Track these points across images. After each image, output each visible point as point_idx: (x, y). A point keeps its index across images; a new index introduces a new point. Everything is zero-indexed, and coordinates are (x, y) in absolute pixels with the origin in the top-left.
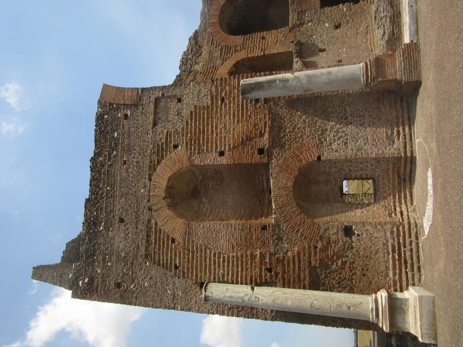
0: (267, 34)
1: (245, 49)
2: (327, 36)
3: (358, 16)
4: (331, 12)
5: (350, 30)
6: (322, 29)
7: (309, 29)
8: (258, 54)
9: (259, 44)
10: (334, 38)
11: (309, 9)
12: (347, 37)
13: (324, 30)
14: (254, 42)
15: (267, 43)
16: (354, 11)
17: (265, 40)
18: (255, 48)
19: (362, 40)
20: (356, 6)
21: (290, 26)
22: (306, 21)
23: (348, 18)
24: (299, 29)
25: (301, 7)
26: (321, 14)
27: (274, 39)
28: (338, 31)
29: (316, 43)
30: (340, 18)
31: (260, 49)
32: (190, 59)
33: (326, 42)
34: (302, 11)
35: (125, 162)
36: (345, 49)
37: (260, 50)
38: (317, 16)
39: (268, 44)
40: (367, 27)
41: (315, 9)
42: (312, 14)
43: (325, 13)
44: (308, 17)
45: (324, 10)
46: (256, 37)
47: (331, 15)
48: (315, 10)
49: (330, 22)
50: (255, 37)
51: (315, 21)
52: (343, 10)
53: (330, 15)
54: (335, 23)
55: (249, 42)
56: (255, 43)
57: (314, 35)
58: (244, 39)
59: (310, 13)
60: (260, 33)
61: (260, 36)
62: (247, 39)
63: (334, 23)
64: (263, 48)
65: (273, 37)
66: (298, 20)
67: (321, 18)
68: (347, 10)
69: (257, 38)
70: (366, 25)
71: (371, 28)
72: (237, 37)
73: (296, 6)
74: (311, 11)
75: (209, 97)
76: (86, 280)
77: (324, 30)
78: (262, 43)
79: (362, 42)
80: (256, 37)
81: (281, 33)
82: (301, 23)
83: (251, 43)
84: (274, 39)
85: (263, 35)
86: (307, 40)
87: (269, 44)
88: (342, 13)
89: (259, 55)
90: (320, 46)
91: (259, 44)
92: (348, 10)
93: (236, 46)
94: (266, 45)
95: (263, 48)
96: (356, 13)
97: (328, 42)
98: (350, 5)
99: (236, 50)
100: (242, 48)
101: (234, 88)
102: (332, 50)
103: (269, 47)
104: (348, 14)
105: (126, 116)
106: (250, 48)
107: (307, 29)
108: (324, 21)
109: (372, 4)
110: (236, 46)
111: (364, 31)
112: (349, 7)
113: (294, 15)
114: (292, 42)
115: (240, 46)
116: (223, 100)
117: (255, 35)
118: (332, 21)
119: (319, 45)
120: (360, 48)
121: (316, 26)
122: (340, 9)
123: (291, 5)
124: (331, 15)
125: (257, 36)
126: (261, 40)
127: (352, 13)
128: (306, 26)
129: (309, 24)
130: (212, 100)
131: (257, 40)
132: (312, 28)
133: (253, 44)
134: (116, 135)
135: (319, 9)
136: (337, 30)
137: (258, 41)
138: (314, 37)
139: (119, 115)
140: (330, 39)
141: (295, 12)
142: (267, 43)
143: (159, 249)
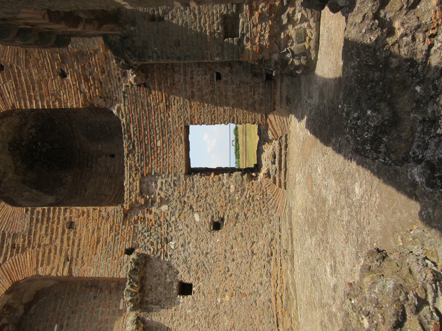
0: (79, 216)
1: (33, 248)
2: (196, 247)
3: (256, 208)
4: (206, 188)
5: (239, 239)
6: (187, 226)
7: (162, 220)
8: (58, 270)
9: (62, 241)
10: (209, 256)
11: (163, 173)
12: (233, 260)
13: (191, 230)
14: (52, 234)
15: (77, 241)
16: (250, 196)
17: (75, 233)
18: (53, 251)
19: (261, 275)
20: (252, 184)
21: (126, 206)
22: (158, 200)
23: (237, 210)
24: (144, 214)
25: (147, 165)
26: (186, 189)
27: (93, 233)
28: (218, 236)
29: (173, 262)
30: (222, 207)
31: (63, 254)
33: (194, 267)
34: (149, 174)
36: (227, 298)
37: (63, 260)
38: (179, 193)
39: (79, 245)
40: (272, 240)
41: (175, 175)
42: (170, 185)
43: (194, 188)
44: (161, 189)
45: (193, 180)
46: (56, 219)
47: (207, 195)
48: (175, 178)
49: (203, 211)
50: (53, 218)
51: (174, 203)
52: (229, 188)
53: (204, 195)
54: (213, 217)
55: (41, 230)
56: (54, 237)
57: (171, 240)
58: (32, 219)
59: (166, 181)
60: (65, 210)
61: (65, 219)
62: (37, 220)
63: (210, 217)
64: (69, 253)
65: (90, 227)
66: (141, 193)
67: (186, 199)
68: (236, 191)
69: (58, 223)
70: (270, 236)
71: (277, 246)
72: (19, 211)
73: (138, 160)
74: (168, 177)
77: (191, 230)
78: (69, 239)
80: (56, 219)
81: (107, 220)
82: (146, 202)
83: (46, 235)
84: (93, 233)
85: (71, 218)
86: (158, 250)
87: (82, 245)
88: (227, 195)
89: (59, 275)
90: (181, 273)
91: (62, 241)
92: (238, 191)
93: (15, 236)
94: (76, 248)
95: (69, 253)
96: (253, 201)
97: (197, 265)
98: (243, 180)
99: (13, 246)
100: (27, 242)
102: (204, 294)
103: (80, 256)
104: (239, 199)
106: (42, 249)
107: (159, 218)
108: (191, 207)
109: (283, 187)
110: (15, 236)
111: (266, 252)
112: (240, 183)
113: (134, 180)
114: (129, 252)
115: (24, 237)
117: (54, 212)
118: (207, 210)
119: (179, 269)
120: (255, 301)
121: (177, 215)
122: (223, 185)
123: (128, 156)
124: (207, 195)
125: (59, 218)
126: (67, 230)
127: (246, 198)
128: (158, 212)
129: (164, 208)
131: (57, 228)
132: (168, 218)
133: (49, 237)
135: (182, 176)
136: (216, 233)
137: (60, 230)
140: (202, 257)
141: (136, 174)
142: (77, 241)
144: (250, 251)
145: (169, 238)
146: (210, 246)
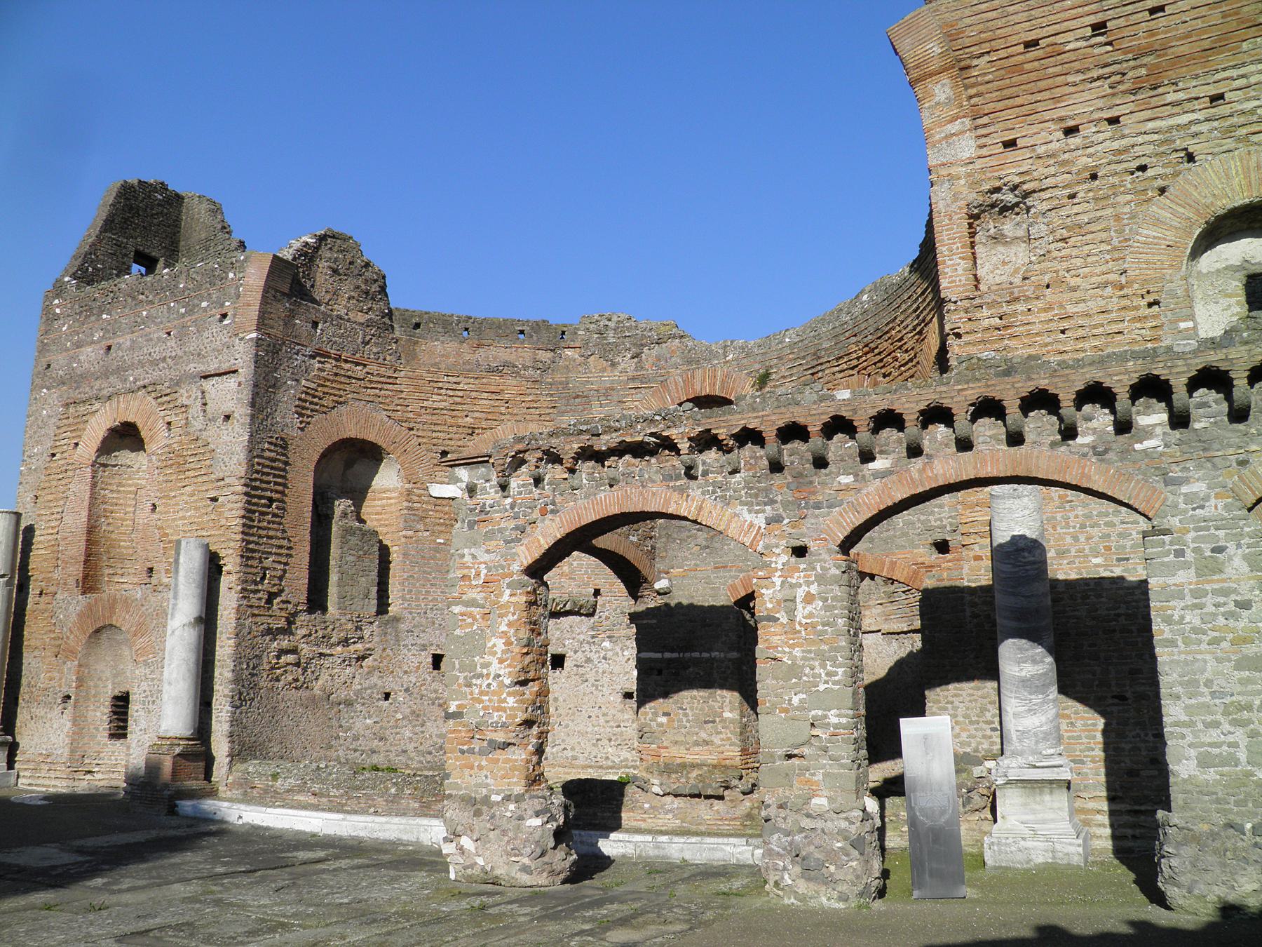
2: (604, 672)
19: (573, 749)
32: (605, 338)
35: (169, 334)
75: (221, 475)
76: (58, 311)
79: (565, 749)
101: (227, 518)
105: (224, 316)
114: (597, 593)
116: (214, 500)
130: (219, 480)
134: (204, 304)
136: (619, 698)
138: (607, 644)
139: (227, 304)
140: (592, 680)
143: (69, 425)
144: (598, 737)
145: (614, 639)
146: (605, 689)
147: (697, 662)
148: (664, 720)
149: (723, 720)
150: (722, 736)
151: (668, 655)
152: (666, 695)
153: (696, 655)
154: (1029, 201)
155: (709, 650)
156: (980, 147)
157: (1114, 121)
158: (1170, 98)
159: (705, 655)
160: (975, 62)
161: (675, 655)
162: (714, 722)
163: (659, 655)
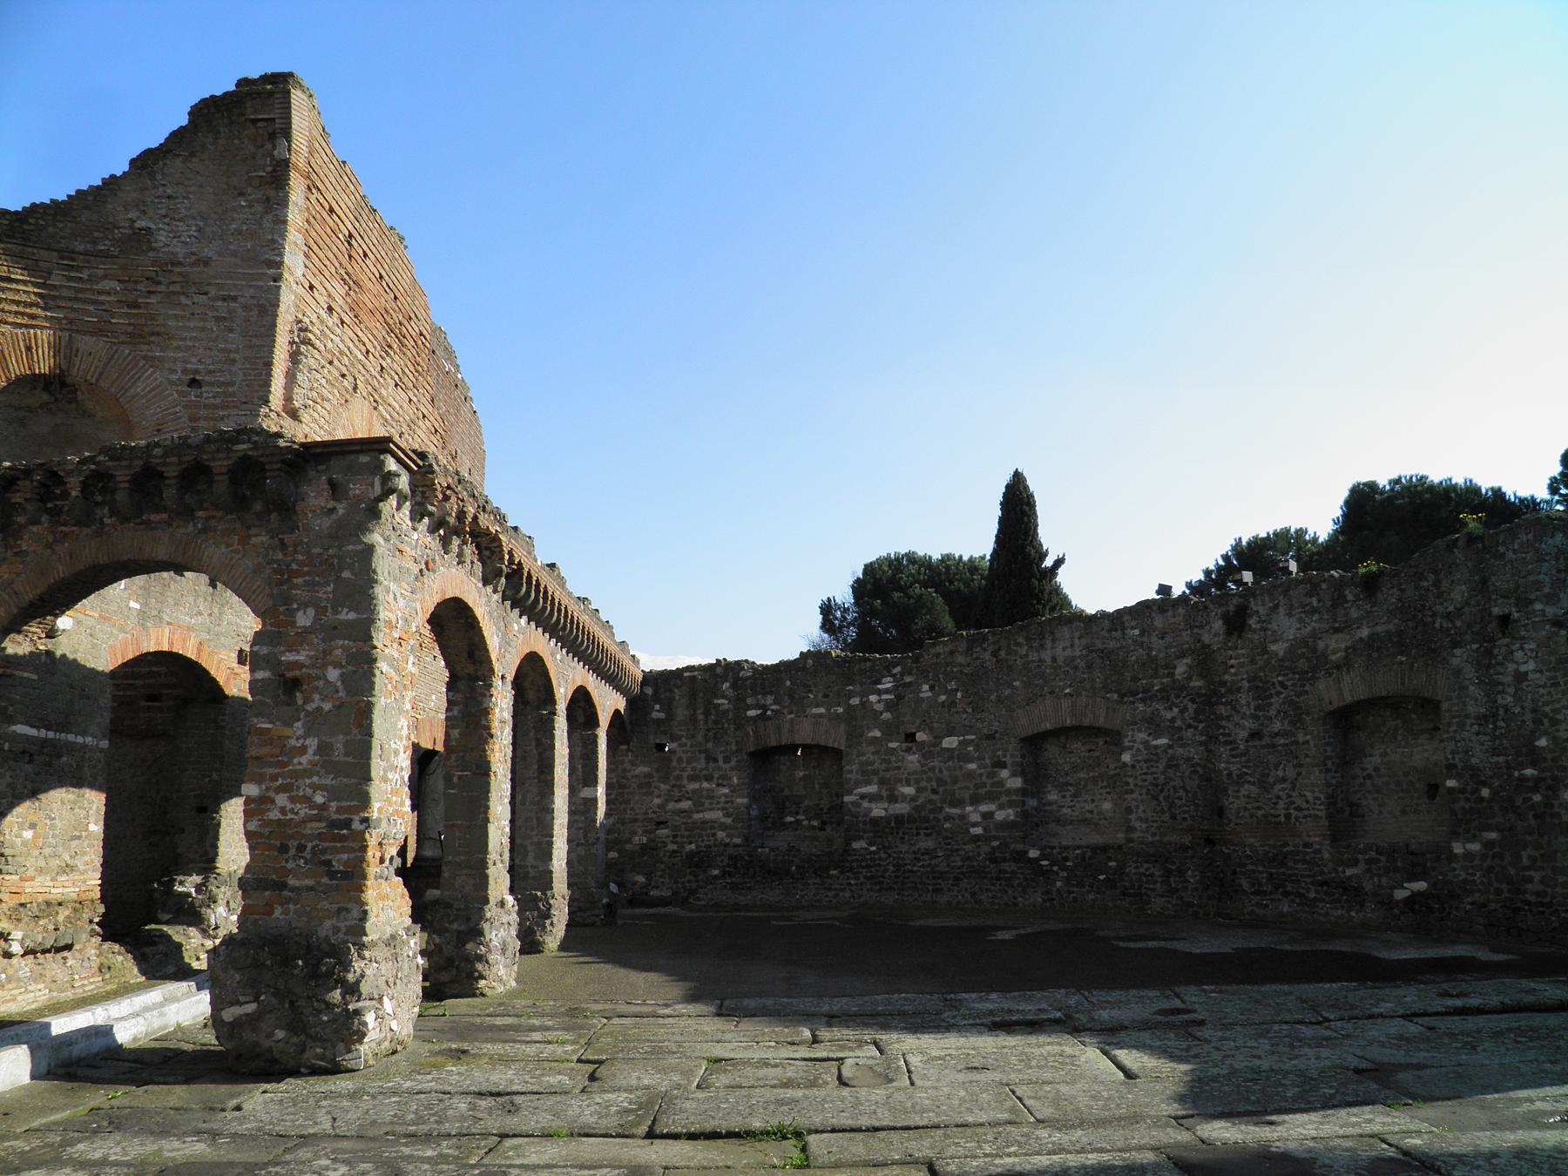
147: (71, 748)
148: (28, 834)
149: (90, 834)
150: (86, 858)
151: (43, 733)
152: (33, 794)
153: (71, 737)
154: (303, 348)
155: (84, 733)
156: (304, 275)
157: (342, 322)
158: (360, 333)
159: (80, 739)
160: (314, 191)
161: (51, 734)
162: (79, 838)
163: (33, 732)
